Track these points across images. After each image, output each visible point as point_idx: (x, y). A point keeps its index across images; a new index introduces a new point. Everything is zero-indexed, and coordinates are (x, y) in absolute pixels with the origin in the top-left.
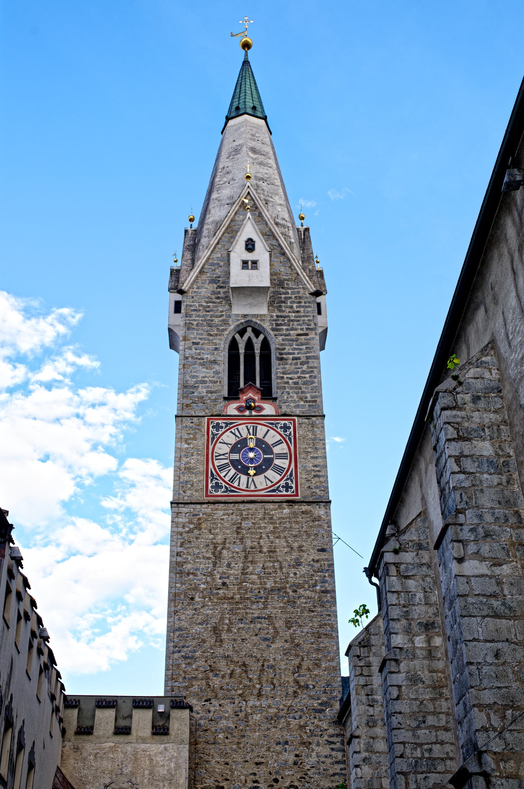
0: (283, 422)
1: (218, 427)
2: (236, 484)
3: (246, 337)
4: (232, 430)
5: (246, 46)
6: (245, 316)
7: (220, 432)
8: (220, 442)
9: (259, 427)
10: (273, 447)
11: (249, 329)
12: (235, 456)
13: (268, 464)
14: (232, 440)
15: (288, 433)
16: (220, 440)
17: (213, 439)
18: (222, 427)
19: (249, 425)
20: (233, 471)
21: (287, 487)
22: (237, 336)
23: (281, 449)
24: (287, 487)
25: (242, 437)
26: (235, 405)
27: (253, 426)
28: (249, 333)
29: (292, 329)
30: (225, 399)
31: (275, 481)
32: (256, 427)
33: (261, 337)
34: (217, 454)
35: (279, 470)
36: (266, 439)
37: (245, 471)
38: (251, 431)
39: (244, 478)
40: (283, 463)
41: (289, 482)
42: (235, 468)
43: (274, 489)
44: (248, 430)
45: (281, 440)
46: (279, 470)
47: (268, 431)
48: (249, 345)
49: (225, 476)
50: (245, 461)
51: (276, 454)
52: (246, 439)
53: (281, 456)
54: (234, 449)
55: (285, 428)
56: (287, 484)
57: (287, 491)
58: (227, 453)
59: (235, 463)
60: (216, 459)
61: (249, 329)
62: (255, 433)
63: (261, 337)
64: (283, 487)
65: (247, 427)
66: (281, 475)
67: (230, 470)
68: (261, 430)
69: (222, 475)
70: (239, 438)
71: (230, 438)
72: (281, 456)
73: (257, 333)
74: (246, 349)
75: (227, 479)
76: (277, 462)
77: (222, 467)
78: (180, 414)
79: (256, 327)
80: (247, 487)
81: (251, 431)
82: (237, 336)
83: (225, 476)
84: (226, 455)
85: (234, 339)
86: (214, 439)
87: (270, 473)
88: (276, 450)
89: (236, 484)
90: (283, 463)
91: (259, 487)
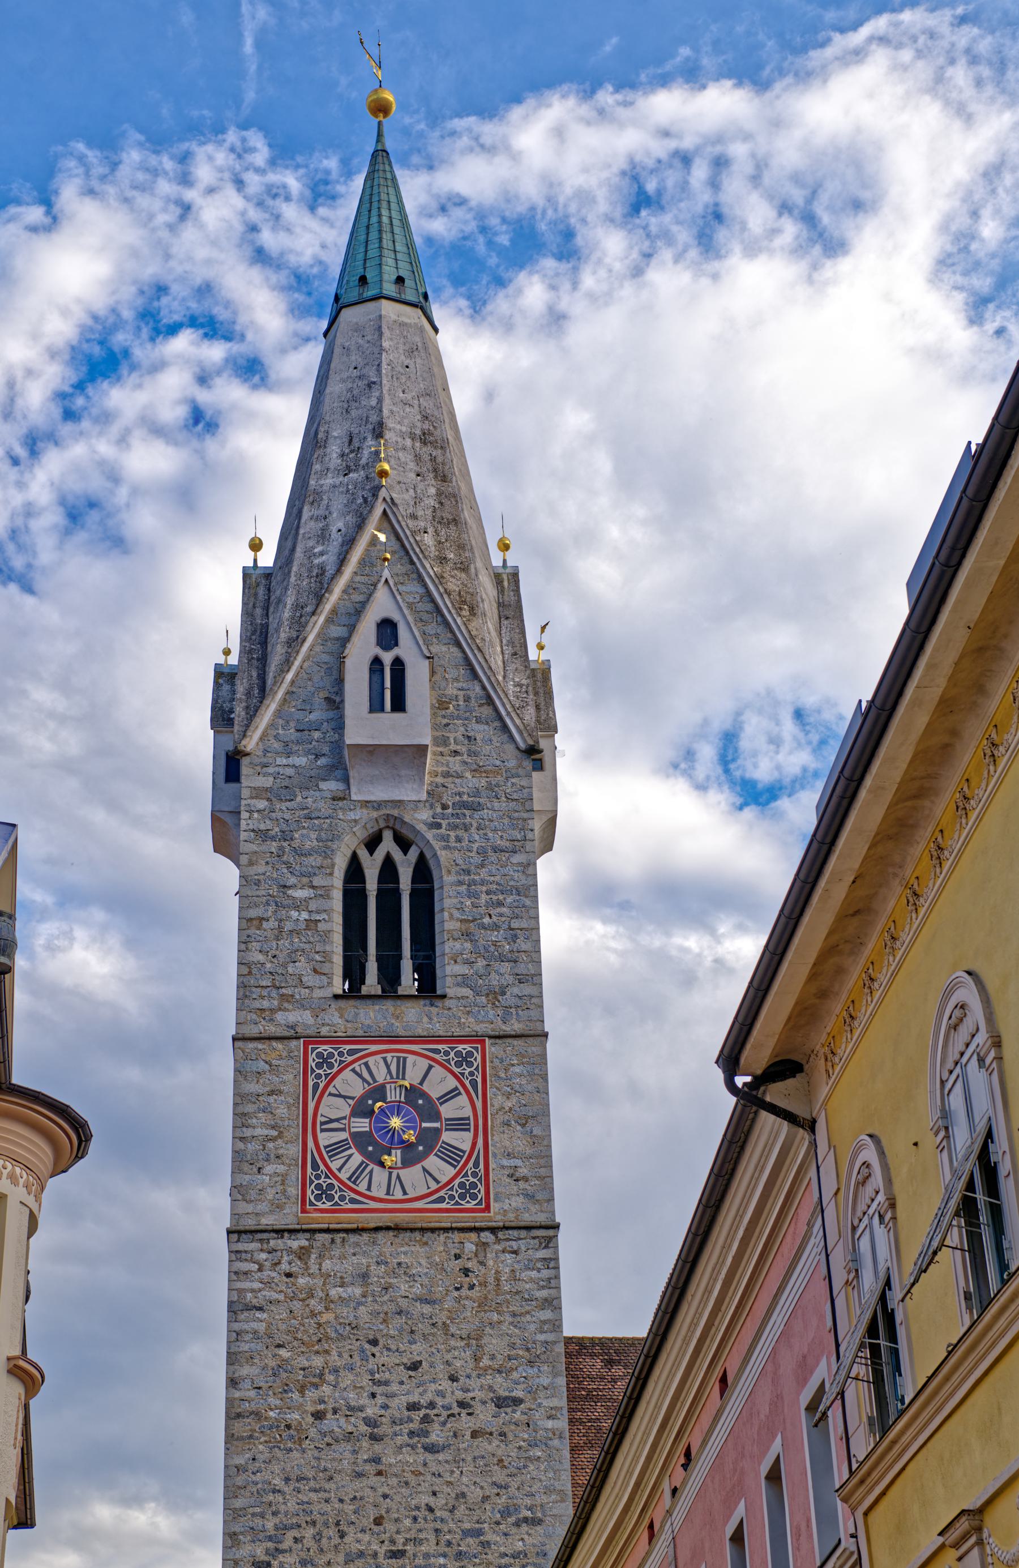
3: (380, 853)
6: (378, 805)
8: (330, 1094)
9: (411, 1059)
10: (441, 1104)
11: (388, 836)
13: (429, 1140)
14: (358, 1089)
19: (389, 1056)
20: (357, 1158)
22: (363, 854)
23: (459, 1108)
25: (375, 1081)
27: (398, 1058)
28: (388, 845)
32: (405, 1059)
33: (413, 854)
34: (324, 1119)
35: (451, 1154)
36: (425, 1087)
38: (393, 1068)
40: (462, 1140)
42: (363, 1152)
45: (456, 1089)
46: (451, 1154)
47: (430, 1067)
48: (389, 869)
49: (340, 1170)
51: (447, 1120)
52: (383, 1087)
53: (459, 1124)
58: (344, 1118)
59: (361, 1140)
60: (322, 1130)
61: (388, 836)
63: (413, 854)
65: (385, 1059)
66: (455, 1167)
67: (350, 1156)
69: (334, 1166)
70: (369, 1084)
72: (459, 1124)
74: (381, 880)
75: (344, 1176)
76: (447, 1137)
79: (405, 831)
80: (388, 1193)
81: (393, 1068)
82: (363, 854)
83: (340, 1170)
84: (344, 1121)
85: (354, 860)
87: (433, 1162)
88: (447, 1111)
89: (362, 1187)
90: (462, 1140)
91: (411, 1195)
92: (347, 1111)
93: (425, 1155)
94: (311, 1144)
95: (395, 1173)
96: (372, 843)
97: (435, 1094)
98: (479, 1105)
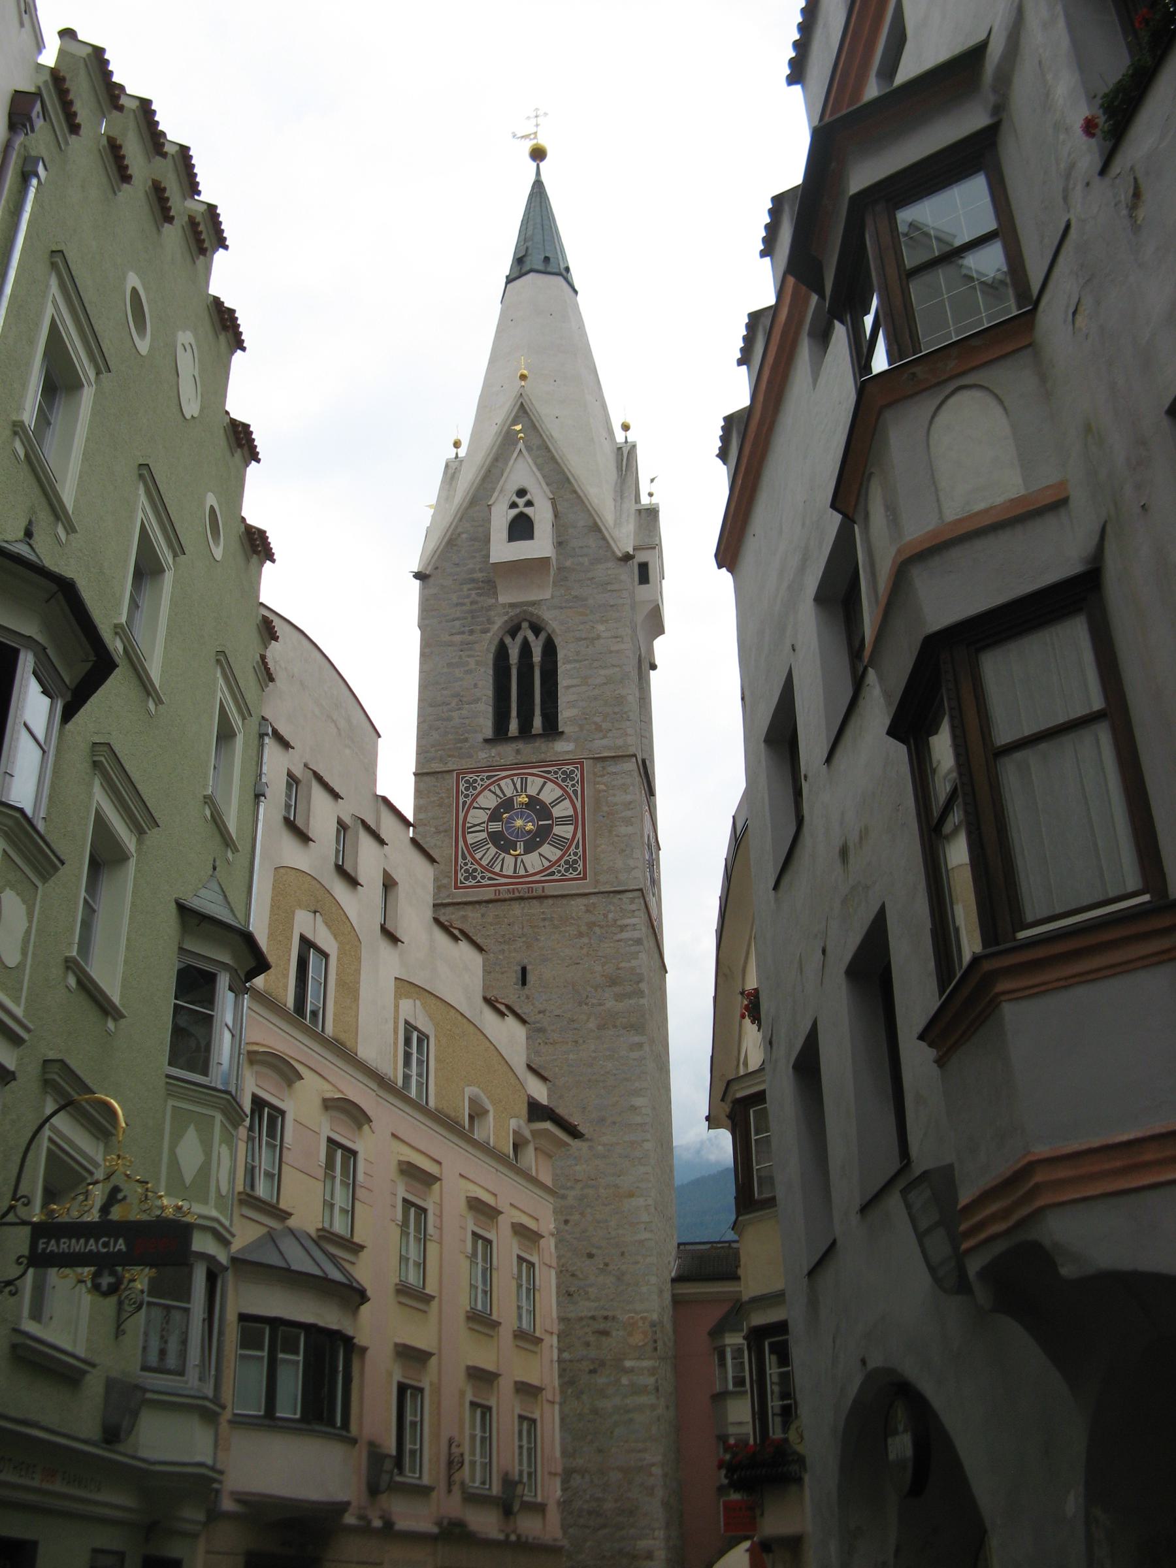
3: (519, 638)
4: (492, 788)
5: (538, 154)
9: (530, 778)
11: (525, 625)
12: (495, 827)
30: (486, 741)
33: (543, 636)
35: (560, 843)
40: (565, 831)
44: (514, 785)
46: (560, 843)
48: (526, 649)
50: (511, 834)
52: (511, 799)
53: (564, 820)
54: (495, 816)
61: (525, 625)
62: (524, 788)
69: (478, 856)
71: (489, 801)
72: (564, 820)
73: (537, 629)
75: (484, 863)
77: (478, 845)
78: (436, 766)
79: (534, 620)
87: (546, 849)
89: (497, 870)
90: (565, 831)
91: (531, 871)
92: (486, 818)
93: (540, 844)
95: (519, 859)
96: (513, 632)
98: (579, 805)
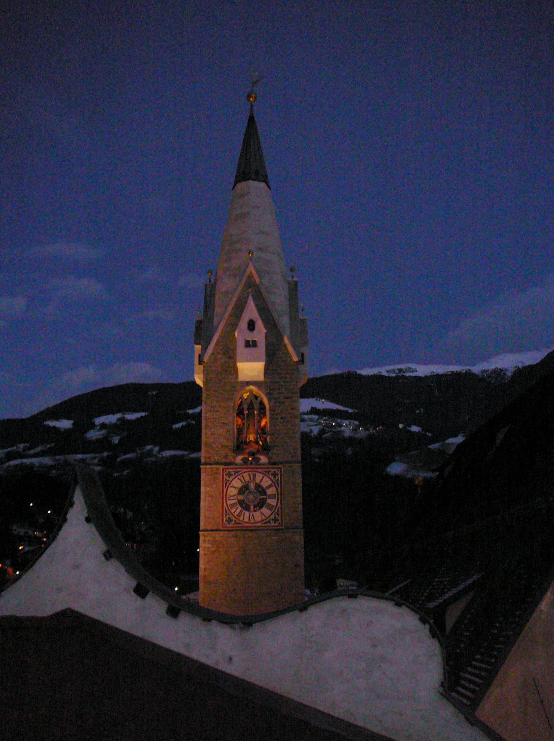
0: (273, 470)
1: (229, 474)
2: (241, 518)
4: (239, 477)
7: (231, 479)
9: (257, 474)
12: (241, 497)
15: (277, 478)
16: (231, 485)
17: (226, 484)
18: (232, 475)
20: (240, 509)
21: (275, 520)
24: (275, 520)
26: (241, 457)
29: (281, 393)
31: (267, 516)
35: (270, 507)
37: (247, 508)
38: (252, 477)
39: (247, 514)
41: (277, 516)
43: (266, 521)
46: (270, 507)
53: (272, 496)
54: (241, 491)
55: (275, 475)
56: (275, 517)
57: (275, 523)
64: (272, 520)
65: (249, 475)
68: (258, 476)
69: (233, 511)
71: (237, 483)
72: (272, 496)
75: (236, 514)
76: (269, 501)
77: (233, 505)
81: (252, 477)
86: (227, 484)
87: (264, 510)
90: (272, 502)
94: (225, 504)
97: (264, 487)
